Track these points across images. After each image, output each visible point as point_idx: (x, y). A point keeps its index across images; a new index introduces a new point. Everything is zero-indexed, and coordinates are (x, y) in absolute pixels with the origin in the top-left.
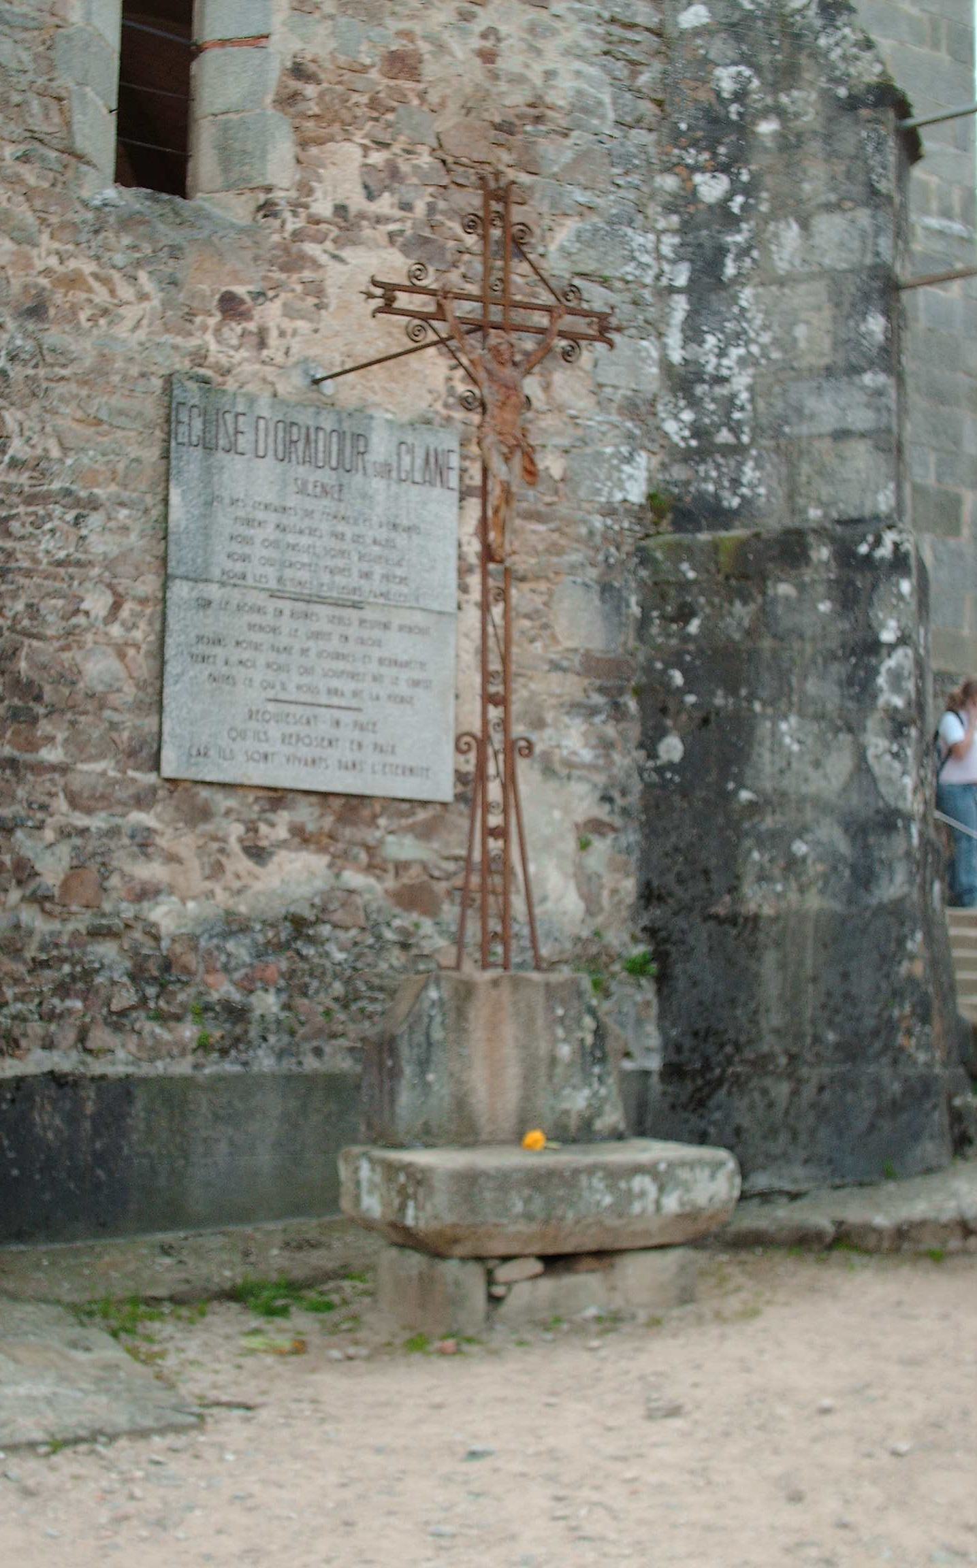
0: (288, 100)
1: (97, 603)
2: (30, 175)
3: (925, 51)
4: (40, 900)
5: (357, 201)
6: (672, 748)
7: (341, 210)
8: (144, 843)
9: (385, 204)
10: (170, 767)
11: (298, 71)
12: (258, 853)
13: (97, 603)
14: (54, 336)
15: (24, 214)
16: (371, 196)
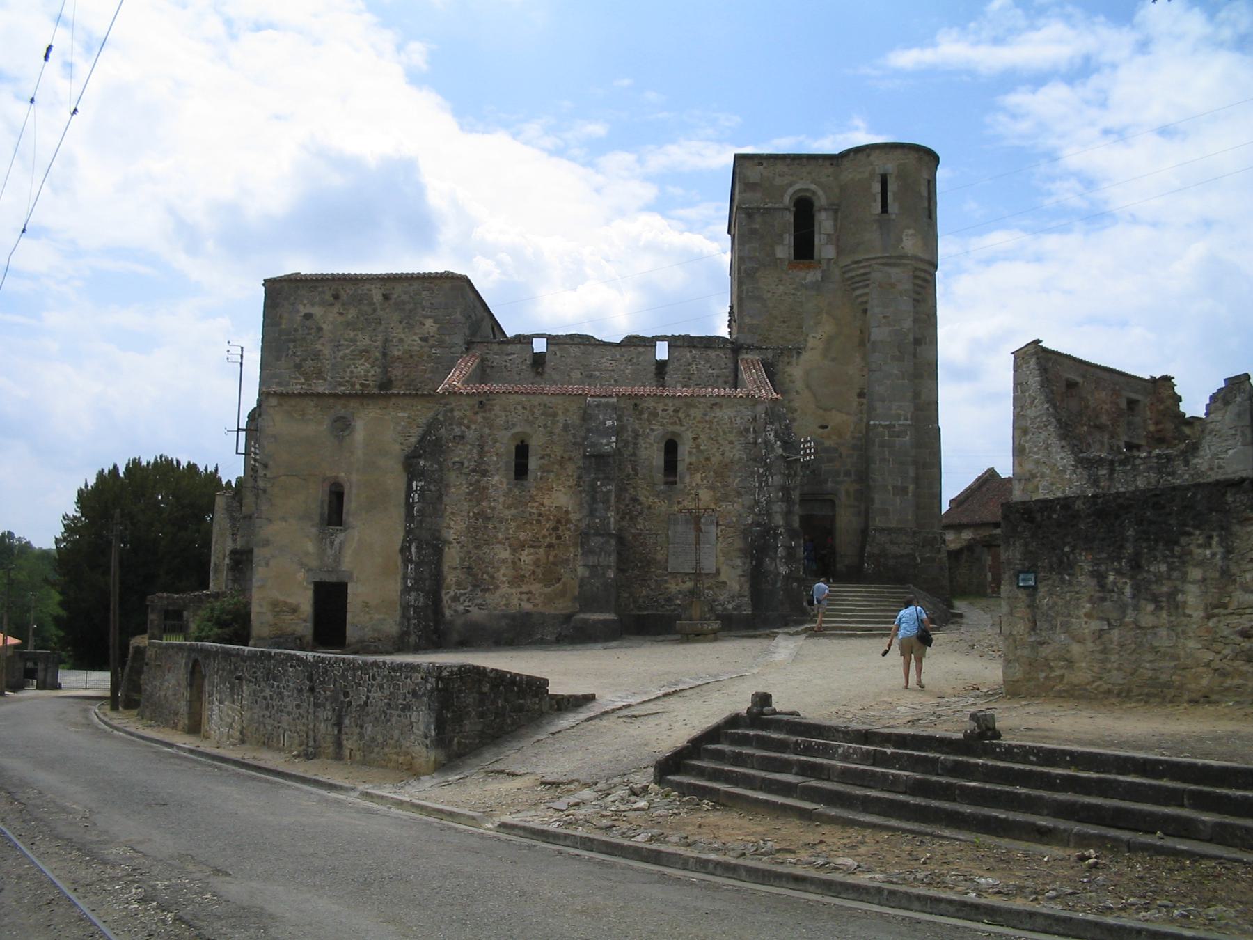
0: (688, 469)
1: (659, 548)
2: (648, 489)
3: (900, 381)
4: (652, 590)
5: (699, 482)
6: (754, 563)
7: (697, 484)
8: (666, 582)
9: (705, 482)
10: (669, 570)
11: (690, 464)
12: (684, 582)
13: (659, 548)
14: (652, 511)
15: (647, 494)
16: (702, 481)
